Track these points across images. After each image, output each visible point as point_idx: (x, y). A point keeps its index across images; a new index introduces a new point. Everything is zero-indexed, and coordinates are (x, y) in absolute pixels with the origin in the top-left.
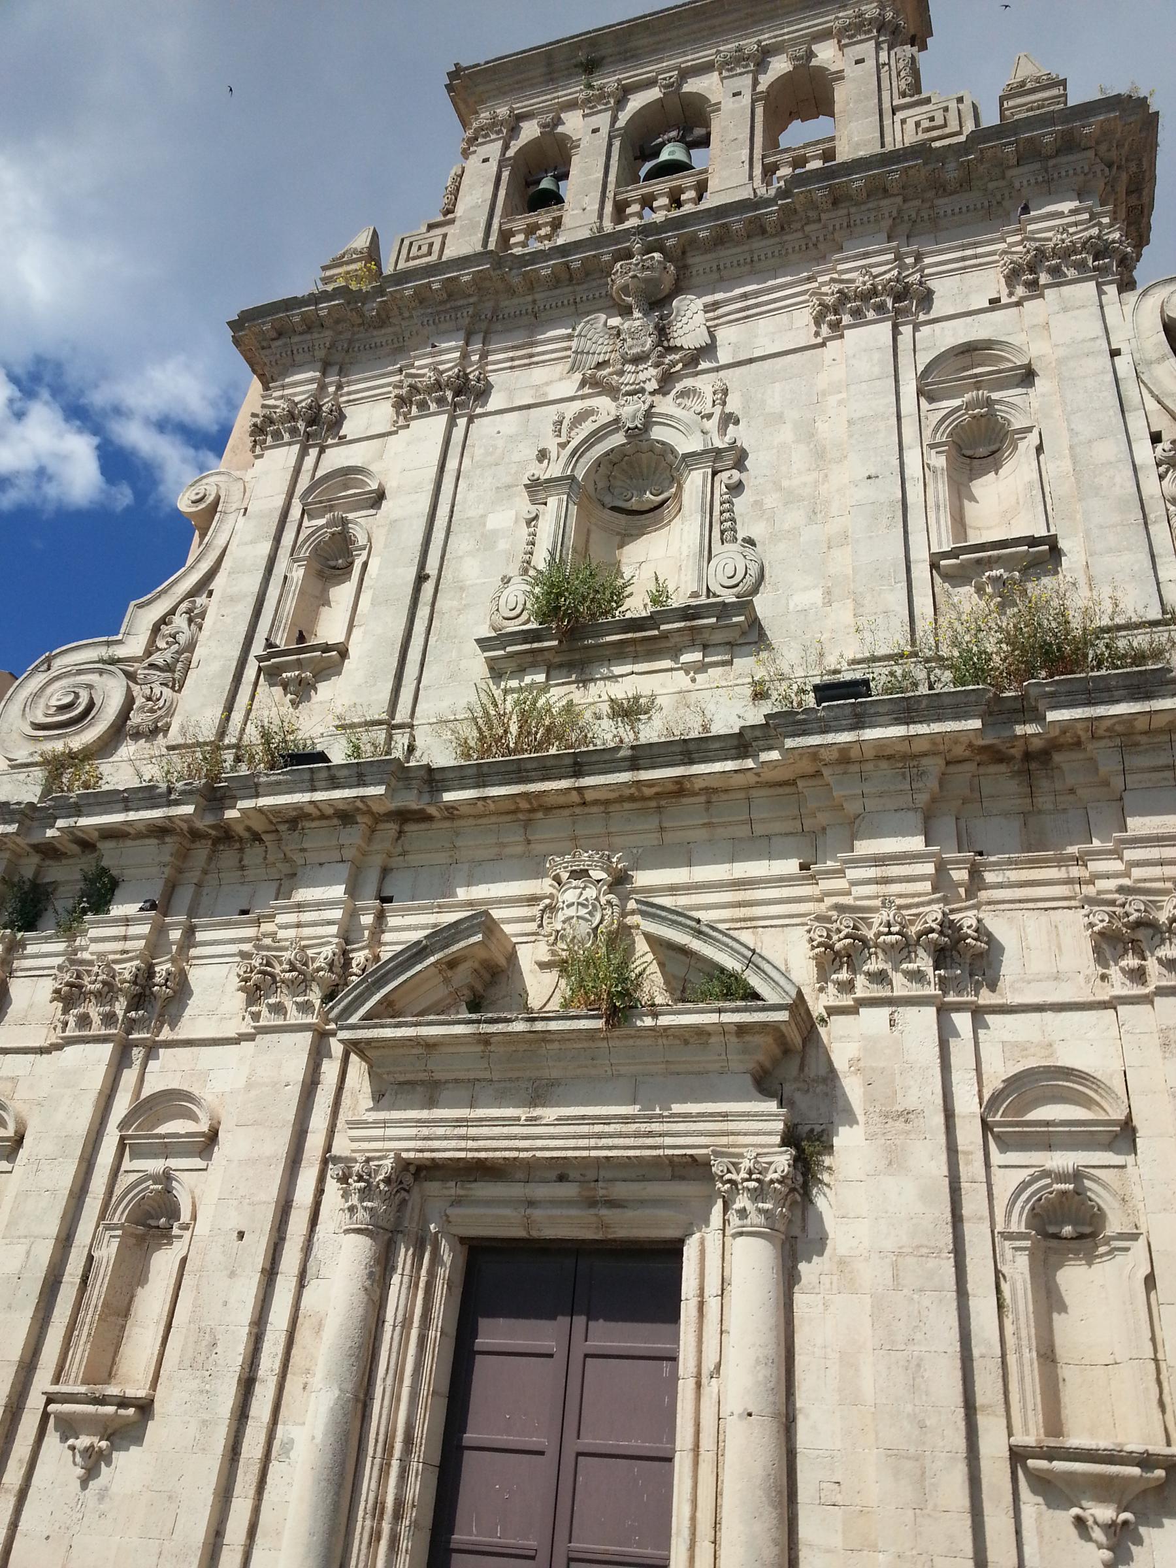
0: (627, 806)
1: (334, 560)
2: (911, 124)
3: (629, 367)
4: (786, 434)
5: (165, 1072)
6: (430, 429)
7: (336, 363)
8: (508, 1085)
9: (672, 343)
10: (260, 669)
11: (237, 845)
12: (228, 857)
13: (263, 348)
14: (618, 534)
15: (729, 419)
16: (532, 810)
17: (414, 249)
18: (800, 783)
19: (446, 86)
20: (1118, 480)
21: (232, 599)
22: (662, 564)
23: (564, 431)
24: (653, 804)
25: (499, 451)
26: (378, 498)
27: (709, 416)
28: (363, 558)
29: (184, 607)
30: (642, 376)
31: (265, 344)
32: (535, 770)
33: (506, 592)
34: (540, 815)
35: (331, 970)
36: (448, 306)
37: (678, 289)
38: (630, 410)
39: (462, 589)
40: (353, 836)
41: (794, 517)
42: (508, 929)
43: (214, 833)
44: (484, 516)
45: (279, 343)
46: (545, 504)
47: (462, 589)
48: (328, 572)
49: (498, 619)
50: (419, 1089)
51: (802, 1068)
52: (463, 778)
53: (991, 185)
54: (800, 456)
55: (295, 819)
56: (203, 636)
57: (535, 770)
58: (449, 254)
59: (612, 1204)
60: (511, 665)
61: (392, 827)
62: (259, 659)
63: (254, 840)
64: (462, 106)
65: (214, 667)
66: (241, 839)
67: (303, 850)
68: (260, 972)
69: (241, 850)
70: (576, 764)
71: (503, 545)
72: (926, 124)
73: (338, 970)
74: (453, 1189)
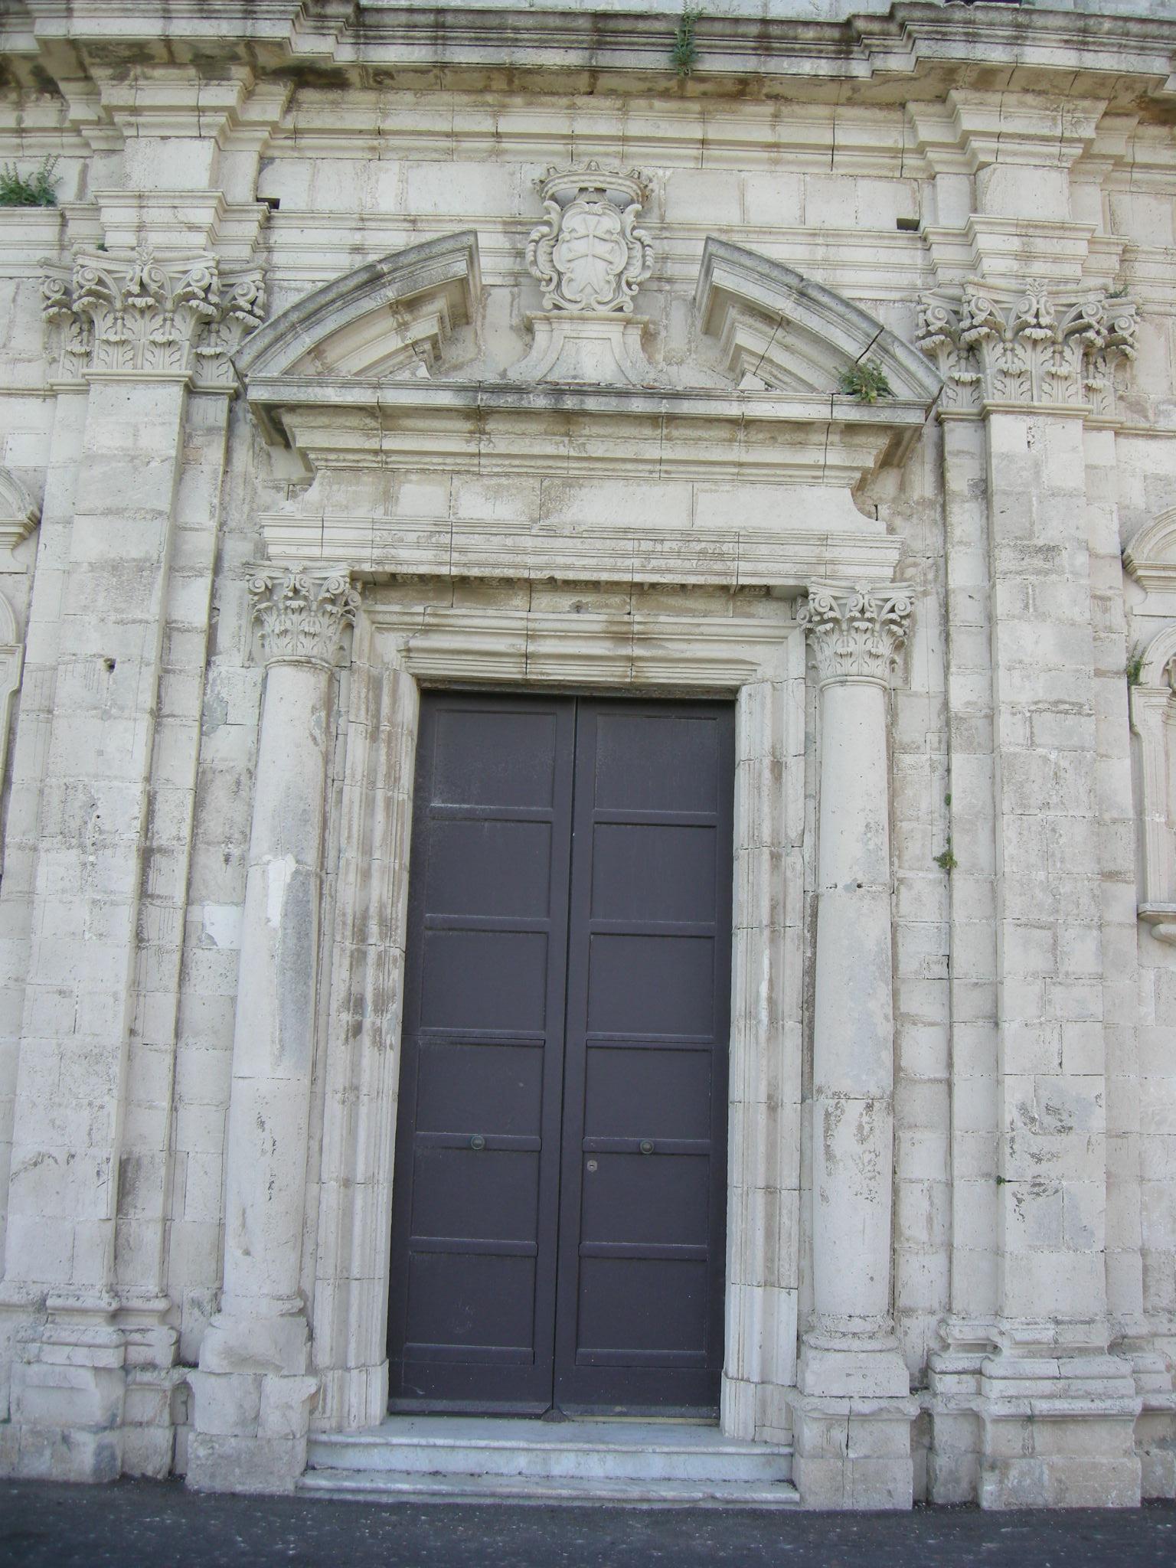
8: (504, 481)
40: (224, 95)
50: (366, 479)
51: (902, 487)
68: (91, 293)
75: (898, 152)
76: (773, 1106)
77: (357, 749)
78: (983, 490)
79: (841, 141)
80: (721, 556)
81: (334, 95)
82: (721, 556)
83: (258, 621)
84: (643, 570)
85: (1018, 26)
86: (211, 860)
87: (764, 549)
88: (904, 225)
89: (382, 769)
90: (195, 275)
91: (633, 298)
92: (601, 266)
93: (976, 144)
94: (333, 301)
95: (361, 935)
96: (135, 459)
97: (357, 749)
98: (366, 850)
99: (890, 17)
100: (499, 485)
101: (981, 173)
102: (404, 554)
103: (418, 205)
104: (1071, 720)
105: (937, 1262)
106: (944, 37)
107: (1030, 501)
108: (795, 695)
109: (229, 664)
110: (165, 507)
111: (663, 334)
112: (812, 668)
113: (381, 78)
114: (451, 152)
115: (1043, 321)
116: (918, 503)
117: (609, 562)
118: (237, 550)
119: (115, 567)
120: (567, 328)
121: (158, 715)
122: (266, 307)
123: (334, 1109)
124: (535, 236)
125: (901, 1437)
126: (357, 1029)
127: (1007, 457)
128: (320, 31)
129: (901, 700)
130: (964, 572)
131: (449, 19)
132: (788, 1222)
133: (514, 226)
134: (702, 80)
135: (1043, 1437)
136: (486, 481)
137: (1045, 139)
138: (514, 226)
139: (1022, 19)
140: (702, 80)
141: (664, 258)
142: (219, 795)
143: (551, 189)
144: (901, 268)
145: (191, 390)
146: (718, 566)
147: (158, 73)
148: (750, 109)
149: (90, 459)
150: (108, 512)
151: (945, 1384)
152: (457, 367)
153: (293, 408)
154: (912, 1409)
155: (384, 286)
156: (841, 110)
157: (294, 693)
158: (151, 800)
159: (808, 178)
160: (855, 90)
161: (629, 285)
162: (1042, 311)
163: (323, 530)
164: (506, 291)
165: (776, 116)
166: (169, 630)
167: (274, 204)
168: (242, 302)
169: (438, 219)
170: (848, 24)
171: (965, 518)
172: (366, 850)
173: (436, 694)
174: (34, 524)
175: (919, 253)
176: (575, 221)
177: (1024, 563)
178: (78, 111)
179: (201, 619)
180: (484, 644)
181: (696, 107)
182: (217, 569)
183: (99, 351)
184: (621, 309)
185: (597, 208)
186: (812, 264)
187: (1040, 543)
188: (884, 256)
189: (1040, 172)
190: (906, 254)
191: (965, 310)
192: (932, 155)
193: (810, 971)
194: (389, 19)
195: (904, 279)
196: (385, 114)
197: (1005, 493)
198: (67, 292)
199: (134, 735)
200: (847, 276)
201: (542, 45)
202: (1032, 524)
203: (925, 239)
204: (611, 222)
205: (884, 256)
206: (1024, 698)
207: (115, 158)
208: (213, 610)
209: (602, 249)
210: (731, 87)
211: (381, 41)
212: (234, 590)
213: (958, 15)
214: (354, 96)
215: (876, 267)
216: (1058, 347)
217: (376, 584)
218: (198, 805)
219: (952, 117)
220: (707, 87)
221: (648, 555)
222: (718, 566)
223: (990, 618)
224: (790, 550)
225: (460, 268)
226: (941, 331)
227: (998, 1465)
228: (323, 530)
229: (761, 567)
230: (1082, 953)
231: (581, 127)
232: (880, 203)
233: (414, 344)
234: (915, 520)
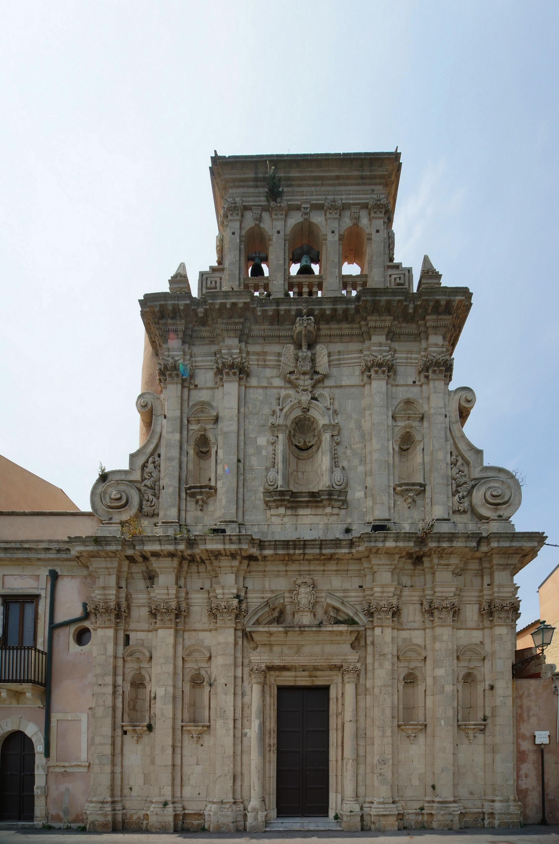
1: (203, 447)
3: (302, 377)
5: (190, 639)
11: (196, 564)
12: (194, 568)
15: (335, 412)
16: (288, 561)
18: (363, 559)
20: (443, 467)
22: (320, 472)
23: (281, 404)
24: (322, 562)
26: (216, 420)
34: (290, 562)
56: (162, 474)
59: (315, 677)
60: (273, 504)
61: (246, 562)
62: (187, 489)
63: (201, 563)
65: (171, 490)
66: (197, 562)
67: (220, 567)
69: (198, 566)
71: (264, 453)
74: (277, 673)
75: (360, 570)
76: (337, 761)
77: (268, 698)
79: (349, 568)
80: (328, 659)
82: (328, 659)
83: (250, 676)
84: (315, 662)
85: (385, 537)
86: (245, 720)
87: (335, 657)
88: (361, 587)
89: (272, 703)
90: (234, 604)
92: (306, 599)
93: (374, 567)
95: (270, 733)
96: (227, 644)
97: (268, 698)
98: (270, 717)
99: (360, 537)
101: (375, 574)
102: (274, 661)
103: (273, 588)
104: (387, 688)
105: (364, 788)
106: (370, 541)
108: (340, 685)
109: (246, 683)
110: (233, 653)
112: (343, 680)
114: (278, 575)
117: (309, 661)
118: (246, 661)
119: (225, 665)
120: (300, 614)
121: (235, 694)
122: (247, 611)
123: (267, 765)
125: (359, 819)
126: (270, 750)
127: (378, 636)
129: (358, 686)
130: (369, 660)
132: (339, 781)
134: (324, 555)
135: (382, 819)
137: (388, 565)
138: (291, 591)
139: (386, 535)
140: (324, 555)
141: (317, 597)
142: (246, 709)
143: (297, 583)
145: (236, 630)
146: (328, 661)
149: (219, 644)
150: (223, 655)
151: (365, 809)
153: (254, 632)
154: (361, 814)
156: (350, 561)
157: (256, 689)
158: (234, 710)
160: (353, 555)
163: (260, 658)
165: (337, 563)
166: (235, 677)
167: (247, 588)
168: (243, 610)
169: (277, 591)
170: (352, 540)
171: (370, 649)
172: (270, 717)
173: (280, 689)
174: (210, 658)
176: (302, 590)
178: (209, 568)
179: (240, 675)
180: (287, 679)
182: (243, 665)
183: (218, 621)
186: (344, 597)
188: (357, 594)
191: (371, 605)
193: (343, 737)
196: (266, 567)
198: (211, 609)
199: (231, 698)
203: (364, 590)
204: (308, 590)
205: (357, 594)
206: (379, 684)
207: (217, 578)
208: (242, 673)
209: (306, 596)
210: (329, 557)
212: (246, 670)
213: (373, 535)
217: (270, 668)
218: (242, 711)
219: (370, 561)
220: (325, 557)
221: (316, 660)
222: (328, 661)
223: (374, 669)
224: (340, 657)
225: (282, 601)
227: (374, 823)
228: (260, 658)
229: (335, 661)
230: (389, 732)
231: (302, 568)
232: (356, 582)
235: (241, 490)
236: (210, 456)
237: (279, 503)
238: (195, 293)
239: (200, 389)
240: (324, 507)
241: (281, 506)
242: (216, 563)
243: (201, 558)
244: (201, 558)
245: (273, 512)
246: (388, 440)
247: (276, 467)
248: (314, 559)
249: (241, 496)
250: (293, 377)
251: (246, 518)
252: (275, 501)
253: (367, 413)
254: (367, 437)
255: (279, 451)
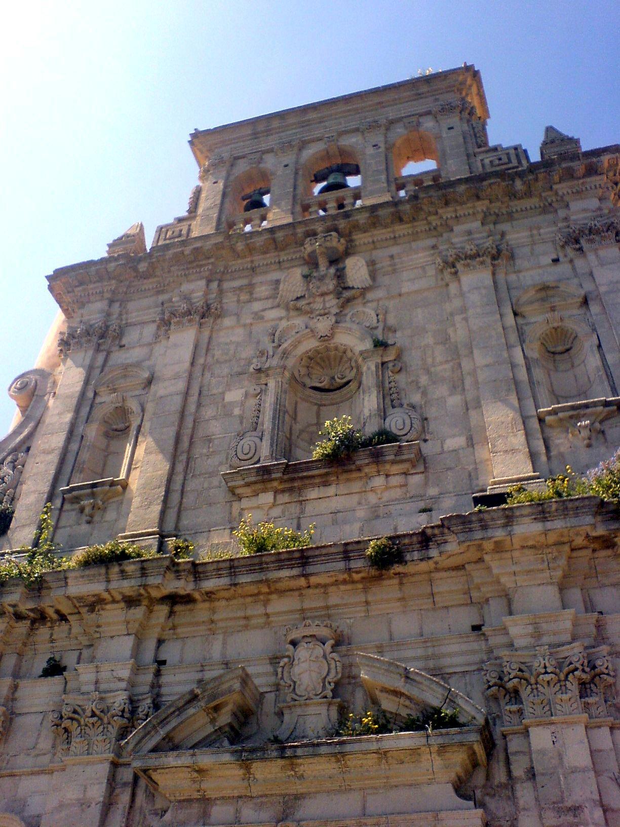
0: (342, 587)
2: (487, 161)
4: (429, 340)
6: (184, 338)
7: (117, 301)
9: (346, 285)
10: (64, 499)
13: (69, 292)
14: (316, 404)
16: (270, 593)
17: (169, 233)
19: (189, 142)
21: (49, 452)
25: (232, 352)
27: (376, 328)
28: (138, 422)
29: (9, 459)
30: (328, 305)
31: (70, 289)
32: (273, 562)
33: (242, 442)
35: (122, 716)
36: (195, 264)
37: (347, 253)
38: (323, 325)
39: (210, 441)
41: (441, 391)
42: (257, 681)
43: (32, 615)
44: (223, 393)
45: (81, 288)
46: (266, 385)
47: (210, 441)
48: (111, 433)
49: (236, 462)
52: (219, 570)
53: (543, 194)
54: (440, 354)
55: (95, 604)
57: (273, 562)
58: (195, 234)
61: (164, 610)
63: (61, 620)
64: (198, 153)
65: (32, 498)
66: (52, 621)
69: (51, 628)
70: (302, 557)
72: (497, 162)
73: (127, 715)
78: (532, 774)
81: (189, 606)
91: (332, 691)
94: (174, 712)
100: (262, 803)
107: (559, 778)
111: (352, 706)
113: (210, 596)
115: (549, 670)
116: (498, 787)
120: (299, 711)
124: (282, 664)
127: (542, 752)
128: (178, 578)
131: (236, 564)
133: (274, 660)
136: (255, 801)
144: (473, 652)
147: (108, 607)
148: (386, 582)
152: (248, 738)
155: (199, 701)
159: (423, 612)
161: (329, 683)
162: (547, 665)
164: (273, 695)
165: (401, 583)
171: (525, 793)
175: (483, 642)
176: (302, 652)
177: (561, 819)
181: (360, 586)
184: (325, 697)
185: (311, 645)
187: (569, 804)
188: (464, 647)
189: (541, 587)
190: (477, 645)
192: (483, 589)
194: (210, 568)
195: (476, 658)
196: (214, 613)
197: (543, 774)
200: (447, 661)
201: (280, 568)
202: (562, 792)
205: (464, 647)
211: (207, 578)
214: (200, 606)
215: (463, 653)
216: (563, 683)
226: (495, 685)
231: (307, 604)
233: (220, 728)
234: (497, 798)
235: (179, 479)
236: (128, 436)
237: (259, 486)
238: (148, 248)
239: (128, 349)
240: (369, 477)
241: (265, 491)
242: (90, 618)
243: (57, 612)
244: (57, 612)
245: (245, 503)
246: (509, 347)
247: (259, 428)
248: (336, 583)
249: (177, 486)
250: (302, 303)
251: (185, 522)
252: (248, 485)
253: (458, 318)
254: (463, 351)
255: (267, 405)
